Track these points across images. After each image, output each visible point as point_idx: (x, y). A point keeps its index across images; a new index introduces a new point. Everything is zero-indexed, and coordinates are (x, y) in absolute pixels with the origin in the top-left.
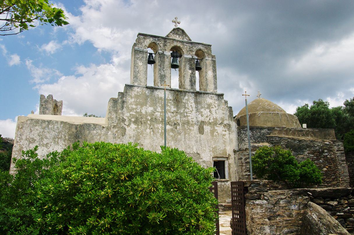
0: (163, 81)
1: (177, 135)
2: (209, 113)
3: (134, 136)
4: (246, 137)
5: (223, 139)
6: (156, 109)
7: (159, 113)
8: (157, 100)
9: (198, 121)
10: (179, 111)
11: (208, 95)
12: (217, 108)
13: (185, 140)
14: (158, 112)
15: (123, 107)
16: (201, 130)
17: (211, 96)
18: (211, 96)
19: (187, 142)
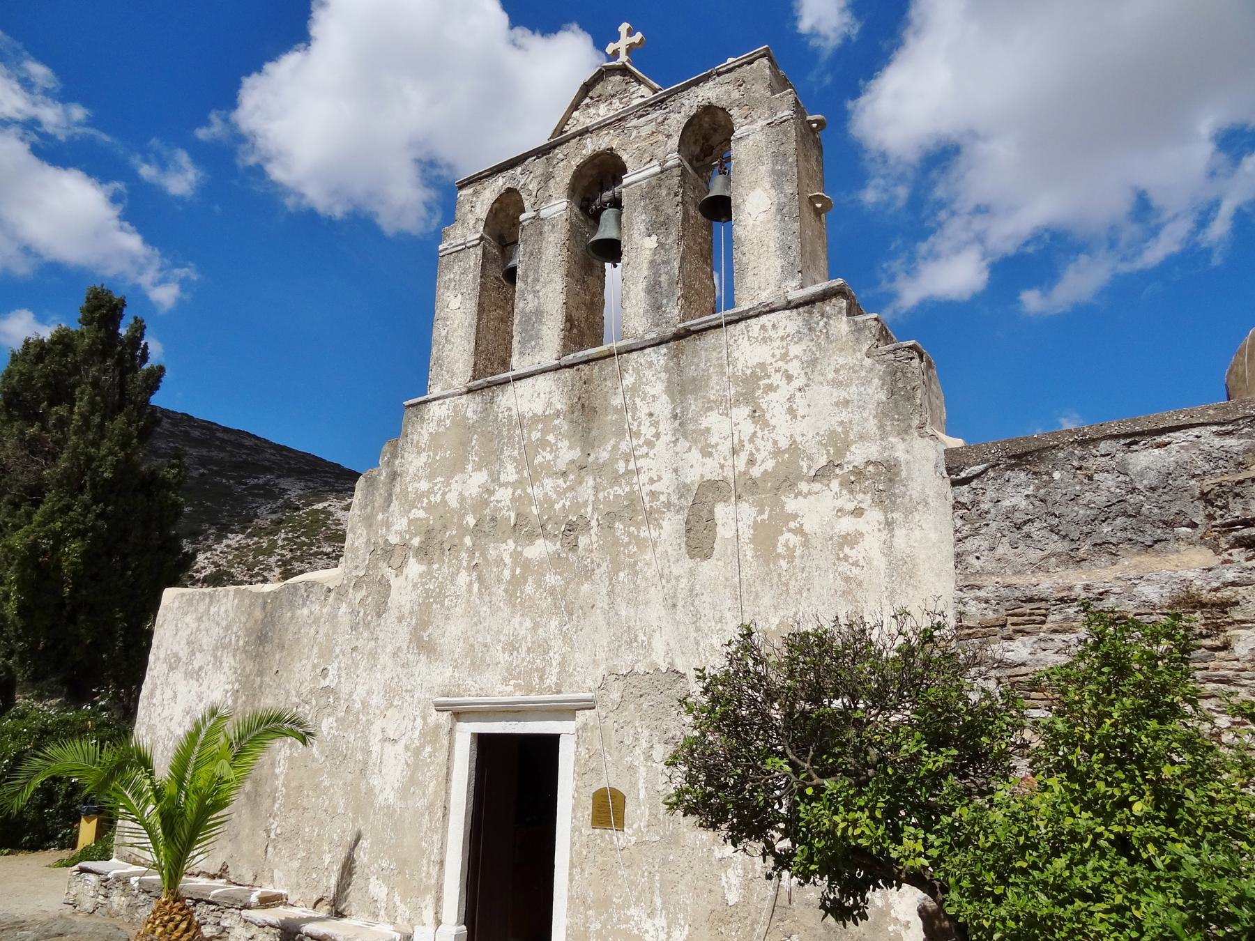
0: (531, 338)
1: (578, 584)
2: (748, 427)
3: (412, 612)
4: (976, 532)
5: (844, 567)
6: (499, 474)
7: (510, 490)
8: (505, 434)
9: (683, 489)
10: (591, 459)
11: (742, 325)
12: (801, 381)
13: (612, 605)
14: (505, 485)
15: (389, 499)
16: (699, 538)
17: (763, 327)
18: (763, 327)
19: (623, 613)
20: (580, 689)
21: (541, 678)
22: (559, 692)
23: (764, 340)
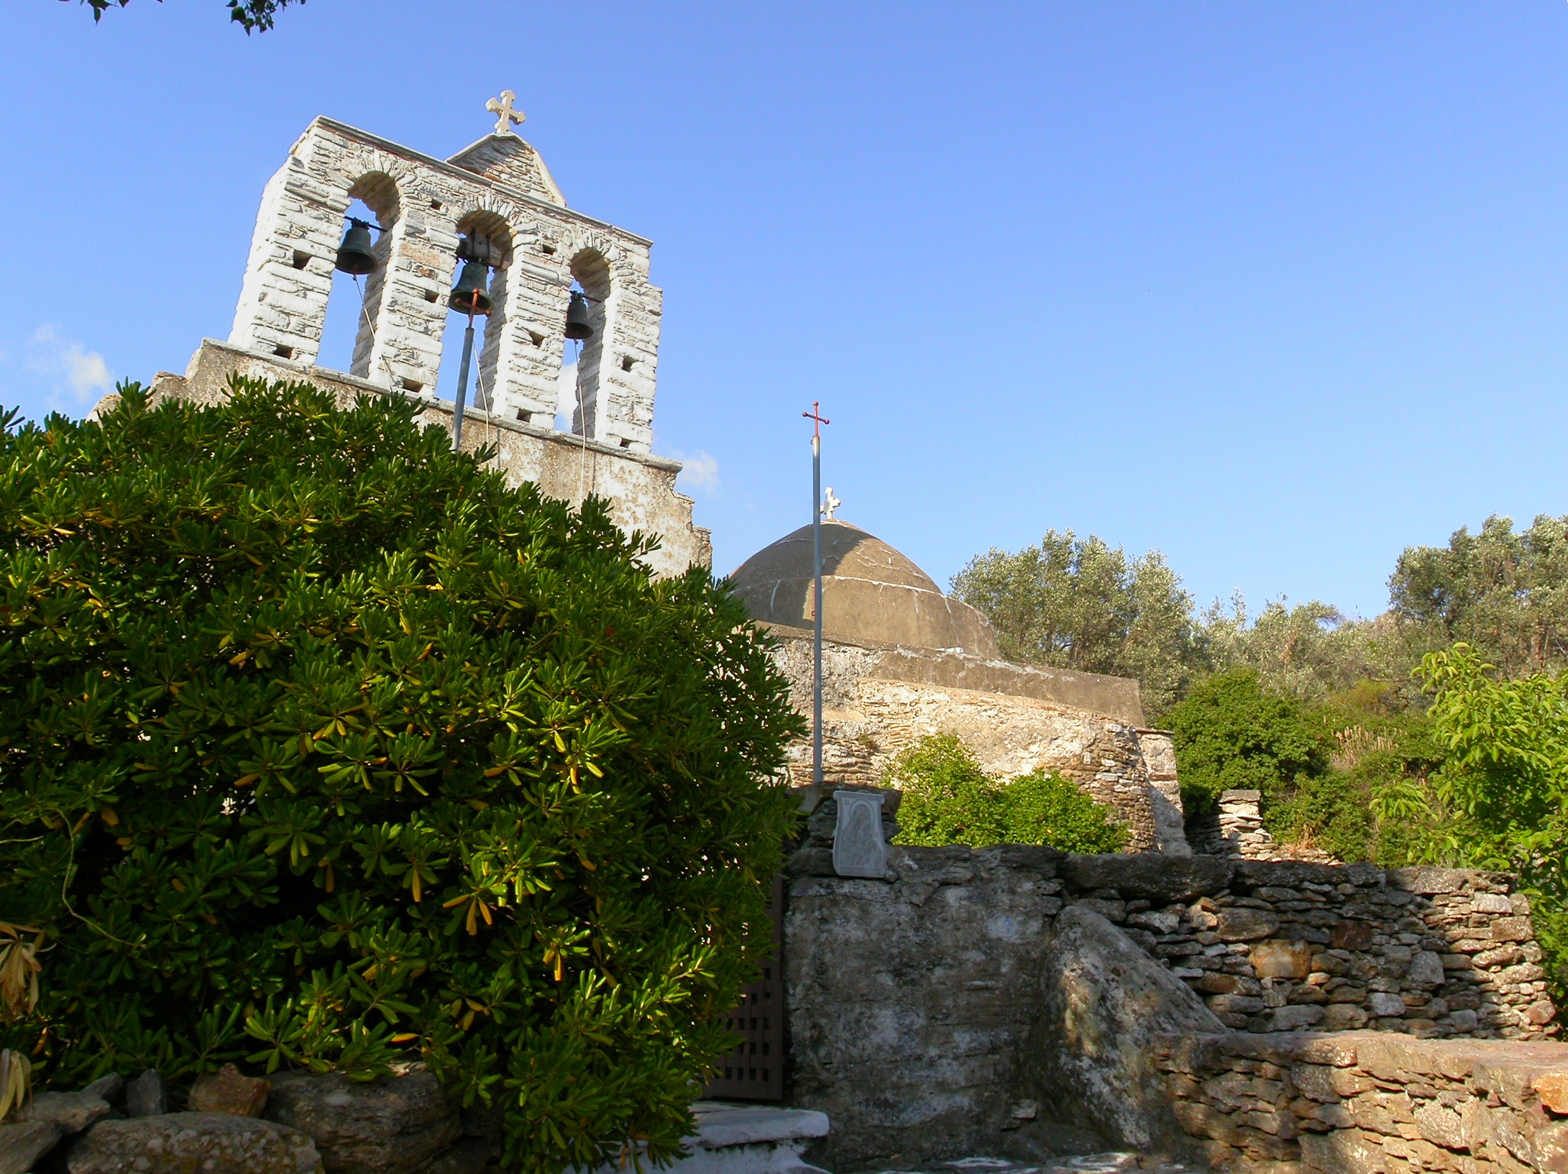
11: (606, 458)
23: (622, 480)
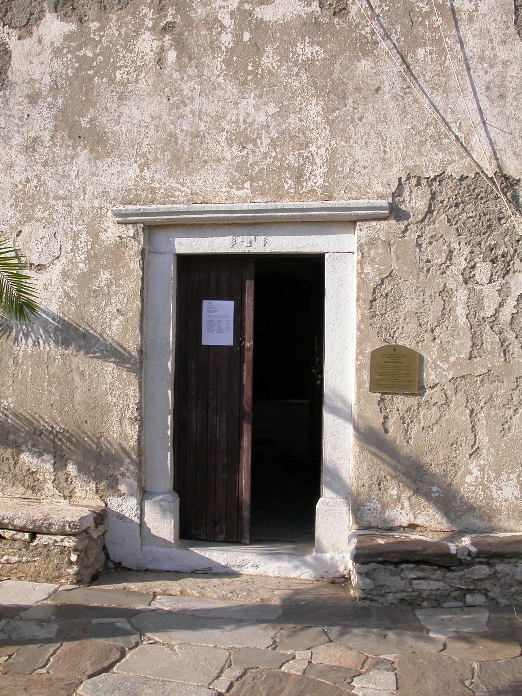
1: (350, 59)
3: (55, 88)
20: (363, 194)
21: (299, 179)
22: (331, 198)
